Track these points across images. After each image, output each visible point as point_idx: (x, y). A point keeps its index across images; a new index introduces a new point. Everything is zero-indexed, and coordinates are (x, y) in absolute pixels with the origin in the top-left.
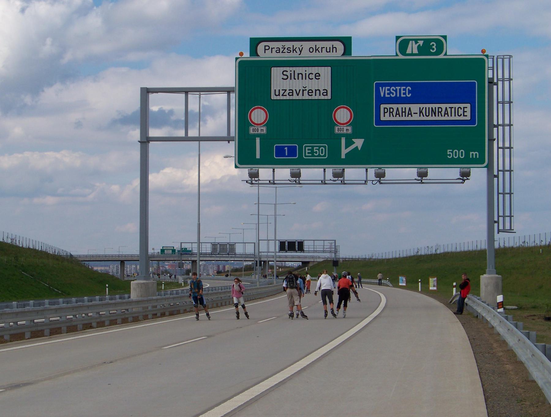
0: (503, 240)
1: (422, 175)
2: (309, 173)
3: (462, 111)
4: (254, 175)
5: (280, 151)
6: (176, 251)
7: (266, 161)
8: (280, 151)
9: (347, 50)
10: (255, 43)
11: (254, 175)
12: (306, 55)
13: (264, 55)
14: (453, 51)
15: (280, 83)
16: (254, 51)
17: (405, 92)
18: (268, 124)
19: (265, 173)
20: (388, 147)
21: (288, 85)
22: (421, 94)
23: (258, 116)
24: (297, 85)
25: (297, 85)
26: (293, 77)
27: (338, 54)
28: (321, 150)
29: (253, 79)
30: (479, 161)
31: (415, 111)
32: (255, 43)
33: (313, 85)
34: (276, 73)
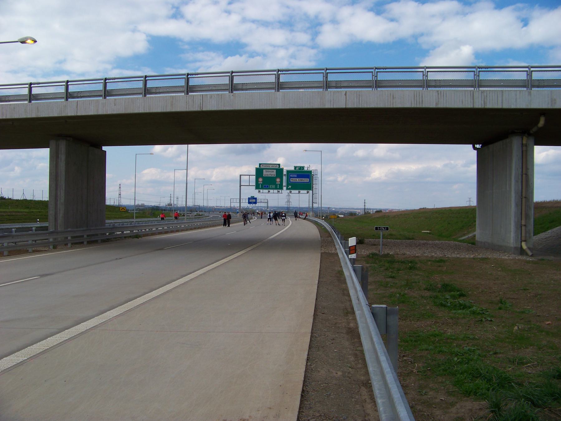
0: (315, 205)
1: (299, 192)
2: (271, 191)
3: (306, 180)
4: (259, 191)
5: (265, 186)
6: (285, 173)
7: (262, 188)
8: (265, 186)
9: (279, 167)
10: (260, 164)
11: (259, 191)
12: (271, 167)
13: (262, 167)
14: (306, 169)
15: (265, 173)
16: (260, 166)
17: (296, 176)
18: (262, 181)
19: (261, 191)
20: (293, 186)
21: (267, 173)
22: (299, 176)
23: (260, 180)
24: (269, 173)
25: (269, 173)
26: (268, 172)
27: (277, 167)
28: (274, 186)
29: (259, 172)
30: (310, 190)
31: (298, 180)
32: (260, 164)
33: (272, 173)
34: (264, 171)
